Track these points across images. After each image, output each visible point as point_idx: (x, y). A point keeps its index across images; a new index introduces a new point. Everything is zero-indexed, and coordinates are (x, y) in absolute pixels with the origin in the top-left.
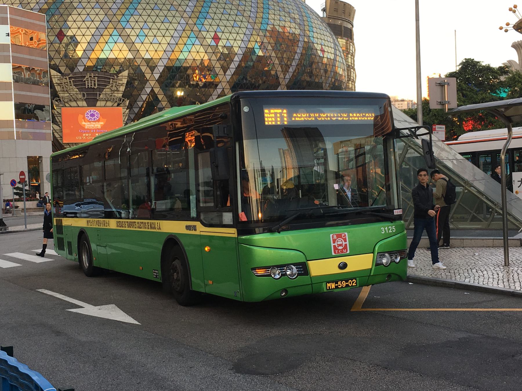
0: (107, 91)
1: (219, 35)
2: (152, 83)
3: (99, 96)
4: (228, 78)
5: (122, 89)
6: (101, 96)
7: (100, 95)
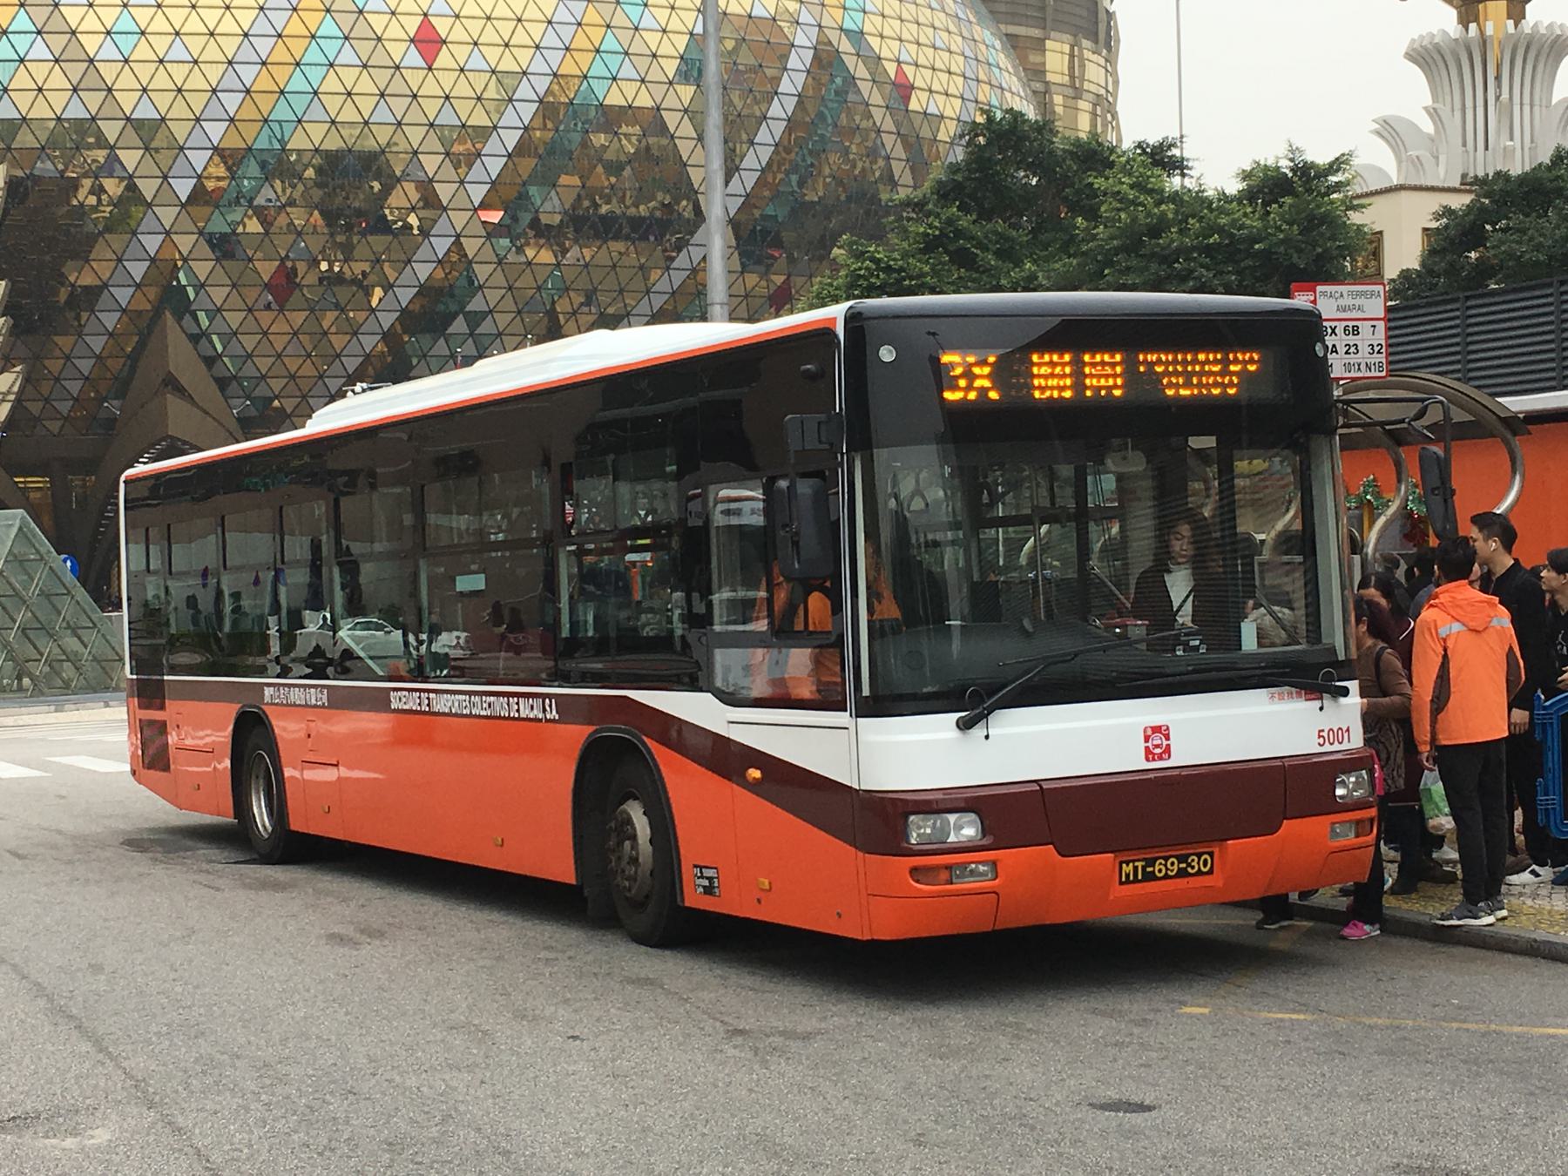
1: (442, 26)
2: (167, 215)
4: (478, 193)
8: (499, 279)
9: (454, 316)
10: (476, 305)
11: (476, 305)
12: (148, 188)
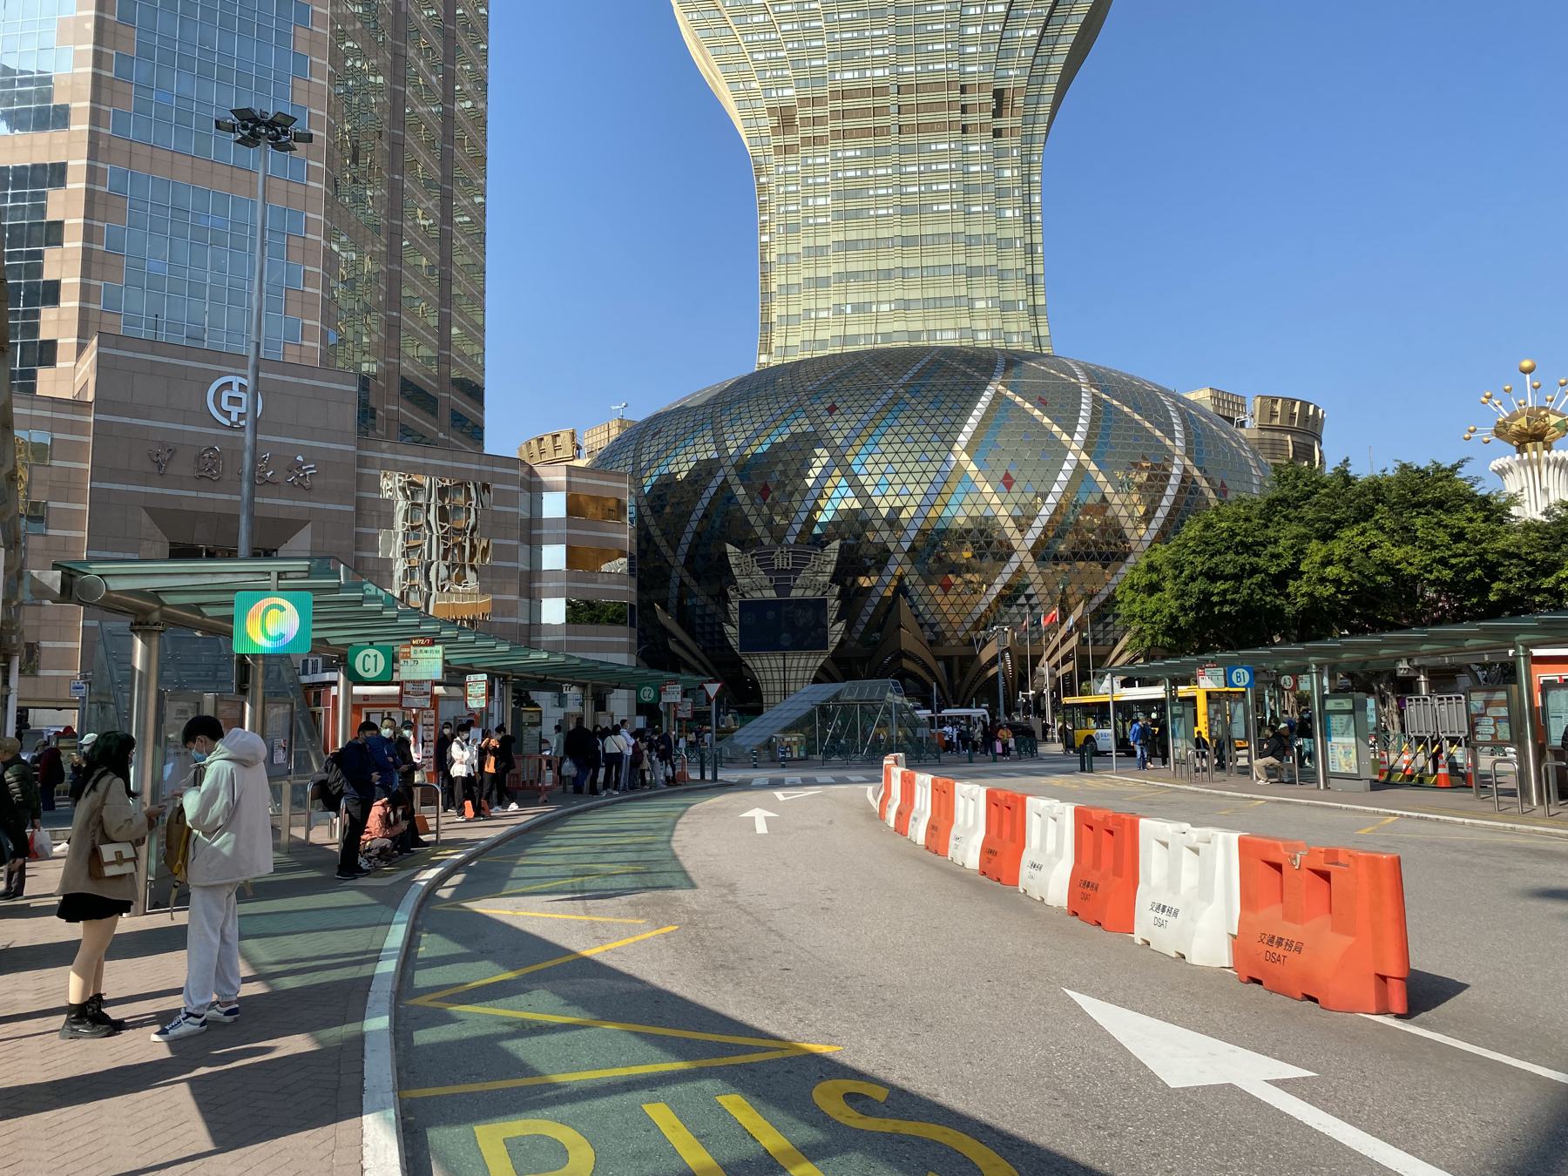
0: (806, 573)
1: (1013, 474)
2: (899, 557)
3: (795, 581)
5: (830, 568)
6: (798, 581)
7: (795, 580)
8: (1040, 580)
9: (1019, 596)
10: (1030, 591)
11: (1030, 591)
12: (892, 546)
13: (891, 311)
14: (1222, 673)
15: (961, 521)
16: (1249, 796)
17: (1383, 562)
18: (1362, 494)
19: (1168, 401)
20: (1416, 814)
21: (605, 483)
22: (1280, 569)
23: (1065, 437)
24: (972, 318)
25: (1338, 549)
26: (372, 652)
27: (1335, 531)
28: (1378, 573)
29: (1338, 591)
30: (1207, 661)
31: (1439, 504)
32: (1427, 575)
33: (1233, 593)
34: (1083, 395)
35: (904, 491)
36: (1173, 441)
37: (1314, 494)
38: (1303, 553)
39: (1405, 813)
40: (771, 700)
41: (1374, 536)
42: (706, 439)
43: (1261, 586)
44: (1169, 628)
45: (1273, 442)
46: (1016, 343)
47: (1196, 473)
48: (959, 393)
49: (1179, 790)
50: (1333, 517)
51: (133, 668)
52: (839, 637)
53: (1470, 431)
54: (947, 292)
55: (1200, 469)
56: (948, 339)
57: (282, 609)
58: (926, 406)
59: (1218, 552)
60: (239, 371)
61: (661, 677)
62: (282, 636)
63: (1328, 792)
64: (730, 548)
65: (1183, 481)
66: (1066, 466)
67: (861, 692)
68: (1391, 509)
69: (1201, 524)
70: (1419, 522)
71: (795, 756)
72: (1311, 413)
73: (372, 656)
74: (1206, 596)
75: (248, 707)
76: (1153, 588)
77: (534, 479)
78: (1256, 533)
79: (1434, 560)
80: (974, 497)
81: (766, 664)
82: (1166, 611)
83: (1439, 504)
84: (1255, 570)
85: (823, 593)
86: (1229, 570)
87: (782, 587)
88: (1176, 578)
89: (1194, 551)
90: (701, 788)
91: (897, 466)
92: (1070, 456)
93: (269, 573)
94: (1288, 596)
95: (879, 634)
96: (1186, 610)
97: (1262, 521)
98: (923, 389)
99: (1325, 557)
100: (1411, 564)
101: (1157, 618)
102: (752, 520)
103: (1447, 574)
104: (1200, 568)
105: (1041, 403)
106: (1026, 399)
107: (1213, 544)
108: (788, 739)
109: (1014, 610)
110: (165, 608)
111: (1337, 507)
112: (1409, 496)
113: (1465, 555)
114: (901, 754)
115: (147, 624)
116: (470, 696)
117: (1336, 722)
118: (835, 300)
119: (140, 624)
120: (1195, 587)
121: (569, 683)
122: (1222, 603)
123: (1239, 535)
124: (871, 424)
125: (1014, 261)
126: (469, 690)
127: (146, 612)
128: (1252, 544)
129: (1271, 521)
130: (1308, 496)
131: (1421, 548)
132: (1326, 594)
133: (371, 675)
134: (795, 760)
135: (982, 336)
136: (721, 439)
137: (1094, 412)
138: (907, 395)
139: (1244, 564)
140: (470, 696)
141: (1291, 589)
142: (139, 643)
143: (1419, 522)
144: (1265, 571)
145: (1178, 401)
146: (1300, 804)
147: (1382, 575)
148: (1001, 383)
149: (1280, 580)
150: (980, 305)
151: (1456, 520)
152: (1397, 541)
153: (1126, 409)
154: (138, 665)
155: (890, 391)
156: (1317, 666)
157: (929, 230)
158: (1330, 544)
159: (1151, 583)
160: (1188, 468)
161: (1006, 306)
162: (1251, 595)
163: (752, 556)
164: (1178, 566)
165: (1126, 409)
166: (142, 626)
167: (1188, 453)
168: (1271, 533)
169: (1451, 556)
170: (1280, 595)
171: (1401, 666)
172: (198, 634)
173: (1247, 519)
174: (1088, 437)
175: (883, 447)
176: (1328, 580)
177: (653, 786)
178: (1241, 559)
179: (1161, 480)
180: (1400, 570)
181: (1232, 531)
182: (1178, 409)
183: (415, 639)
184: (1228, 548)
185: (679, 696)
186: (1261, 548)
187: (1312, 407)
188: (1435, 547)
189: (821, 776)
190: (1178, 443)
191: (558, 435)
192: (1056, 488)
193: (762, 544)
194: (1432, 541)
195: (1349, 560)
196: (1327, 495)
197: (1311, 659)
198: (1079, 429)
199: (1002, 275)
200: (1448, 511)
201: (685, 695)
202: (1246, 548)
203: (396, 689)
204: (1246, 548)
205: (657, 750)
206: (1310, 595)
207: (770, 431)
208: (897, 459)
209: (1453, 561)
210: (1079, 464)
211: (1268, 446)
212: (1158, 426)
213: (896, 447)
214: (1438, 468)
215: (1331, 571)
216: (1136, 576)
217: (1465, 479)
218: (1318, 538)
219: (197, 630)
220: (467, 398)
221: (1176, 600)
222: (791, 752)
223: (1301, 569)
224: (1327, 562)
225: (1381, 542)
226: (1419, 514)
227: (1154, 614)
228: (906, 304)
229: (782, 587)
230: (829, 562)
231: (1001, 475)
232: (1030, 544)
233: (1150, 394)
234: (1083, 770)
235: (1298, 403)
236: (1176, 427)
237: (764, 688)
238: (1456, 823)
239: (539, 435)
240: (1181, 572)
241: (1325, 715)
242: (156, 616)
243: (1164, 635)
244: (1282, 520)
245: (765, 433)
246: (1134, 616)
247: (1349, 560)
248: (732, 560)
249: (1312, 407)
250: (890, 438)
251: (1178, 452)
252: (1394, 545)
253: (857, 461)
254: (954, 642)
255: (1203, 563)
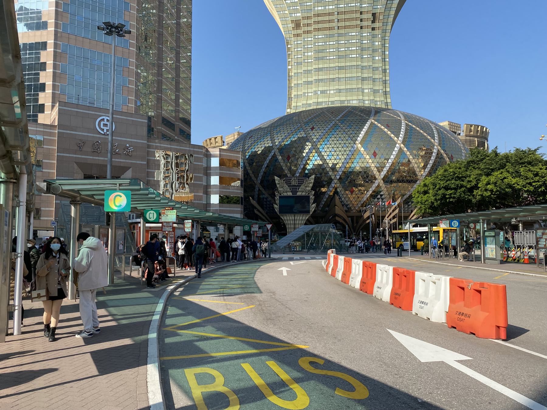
1: (377, 152)
2: (336, 181)
3: (298, 189)
5: (311, 185)
6: (300, 190)
7: (299, 189)
8: (385, 189)
10: (382, 193)
11: (382, 193)
12: (333, 177)
13: (334, 93)
14: (448, 222)
15: (358, 168)
16: (457, 265)
17: (508, 184)
18: (502, 159)
19: (433, 126)
20: (516, 272)
21: (232, 155)
22: (471, 186)
23: (396, 139)
24: (363, 96)
25: (492, 179)
26: (152, 212)
27: (491, 172)
28: (506, 188)
29: (492, 194)
30: (443, 218)
31: (530, 163)
32: (524, 189)
33: (454, 195)
34: (403, 123)
35: (338, 158)
36: (434, 140)
37: (484, 159)
38: (480, 180)
39: (512, 272)
40: (290, 230)
41: (505, 174)
42: (268, 139)
43: (464, 192)
44: (431, 206)
45: (470, 141)
46: (379, 105)
47: (442, 152)
48: (358, 122)
49: (432, 263)
50: (491, 168)
51: (71, 216)
52: (314, 209)
53: (542, 137)
54: (354, 86)
55: (444, 150)
56: (355, 103)
57: (121, 196)
58: (346, 127)
59: (449, 180)
60: (107, 115)
61: (251, 222)
62: (121, 206)
63: (485, 264)
64: (276, 178)
65: (437, 154)
66: (396, 149)
67: (321, 228)
68: (512, 165)
69: (443, 170)
70: (522, 169)
71: (298, 250)
72: (484, 130)
73: (152, 213)
74: (444, 195)
75: (110, 230)
76: (425, 193)
77: (208, 153)
78: (463, 173)
79: (527, 183)
80: (363, 160)
81: (288, 218)
82: (430, 201)
83: (530, 163)
84: (462, 186)
85: (308, 194)
86: (453, 186)
87: (294, 191)
88: (434, 189)
89: (440, 179)
90: (265, 260)
91: (335, 149)
92: (397, 145)
93: (116, 184)
94: (473, 195)
95: (328, 208)
96: (437, 200)
97: (465, 169)
98: (345, 121)
99: (488, 182)
100: (518, 185)
101: (427, 203)
102: (284, 168)
103: (532, 189)
104: (442, 186)
105: (387, 126)
106: (382, 125)
107: (447, 177)
108: (295, 244)
109: (376, 200)
110: (82, 196)
111: (492, 164)
112: (519, 160)
113: (538, 181)
114: (334, 250)
115: (75, 201)
116: (186, 227)
117: (488, 240)
118: (314, 89)
119: (73, 201)
120: (440, 192)
121: (220, 223)
122: (450, 198)
123: (456, 174)
124: (327, 134)
125: (378, 75)
126: (185, 225)
127: (75, 197)
128: (461, 177)
129: (468, 169)
130: (482, 160)
131: (522, 179)
132: (487, 195)
133: (152, 220)
134: (298, 251)
135: (367, 102)
136: (273, 139)
137: (406, 129)
138: (340, 123)
139: (458, 184)
140: (186, 227)
141: (475, 193)
142: (73, 208)
143: (522, 169)
144: (466, 187)
145: (436, 126)
146: (474, 268)
147: (508, 188)
148: (373, 119)
149: (471, 190)
150: (366, 91)
151: (536, 169)
152: (514, 176)
153: (418, 129)
154: (73, 215)
155: (334, 122)
156: (482, 220)
157: (348, 64)
158: (489, 177)
159: (425, 191)
160: (439, 150)
161: (375, 92)
162: (460, 195)
163: (284, 180)
164: (434, 185)
165: (418, 129)
166: (74, 202)
167: (439, 144)
168: (468, 173)
169: (533, 182)
170: (471, 195)
171: (513, 220)
172: (93, 205)
173: (460, 168)
174: (404, 138)
175: (331, 142)
176: (488, 190)
177: (248, 259)
178: (457, 182)
179: (430, 154)
180: (514, 187)
181: (454, 172)
182: (436, 128)
183: (167, 207)
184: (453, 178)
185: (258, 229)
186: (464, 179)
187: (485, 128)
188: (527, 179)
189: (306, 257)
190: (436, 141)
191: (217, 138)
192: (392, 157)
193: (287, 176)
194: (526, 176)
195: (496, 183)
196: (489, 160)
197: (480, 217)
198: (401, 135)
199: (374, 80)
200: (533, 166)
201: (259, 228)
202: (459, 178)
203: (160, 225)
204: (459, 178)
205: (250, 247)
206: (482, 195)
207: (290, 136)
208: (335, 146)
209: (534, 184)
210: (400, 148)
211: (468, 142)
212: (429, 135)
213: (335, 142)
214: (530, 150)
215: (490, 187)
216: (419, 188)
217: (539, 154)
218: (485, 175)
219: (92, 203)
220: (185, 125)
221: (434, 197)
222: (296, 248)
223: (479, 186)
224: (488, 183)
225: (508, 176)
226: (522, 166)
227: (426, 201)
228: (340, 91)
229: (294, 191)
230: (311, 183)
231: (373, 152)
232: (382, 177)
233: (427, 123)
234: (398, 256)
235: (480, 127)
236: (435, 135)
237: (287, 226)
238: (529, 275)
239: (210, 138)
240: (436, 187)
241: (485, 237)
242: (78, 199)
243: (429, 209)
244: (472, 169)
245: (289, 137)
246: (419, 202)
247: (496, 183)
248: (277, 182)
249: (485, 128)
250: (333, 139)
251: (436, 144)
252: (512, 178)
253: (321, 147)
254: (354, 211)
255: (444, 184)
